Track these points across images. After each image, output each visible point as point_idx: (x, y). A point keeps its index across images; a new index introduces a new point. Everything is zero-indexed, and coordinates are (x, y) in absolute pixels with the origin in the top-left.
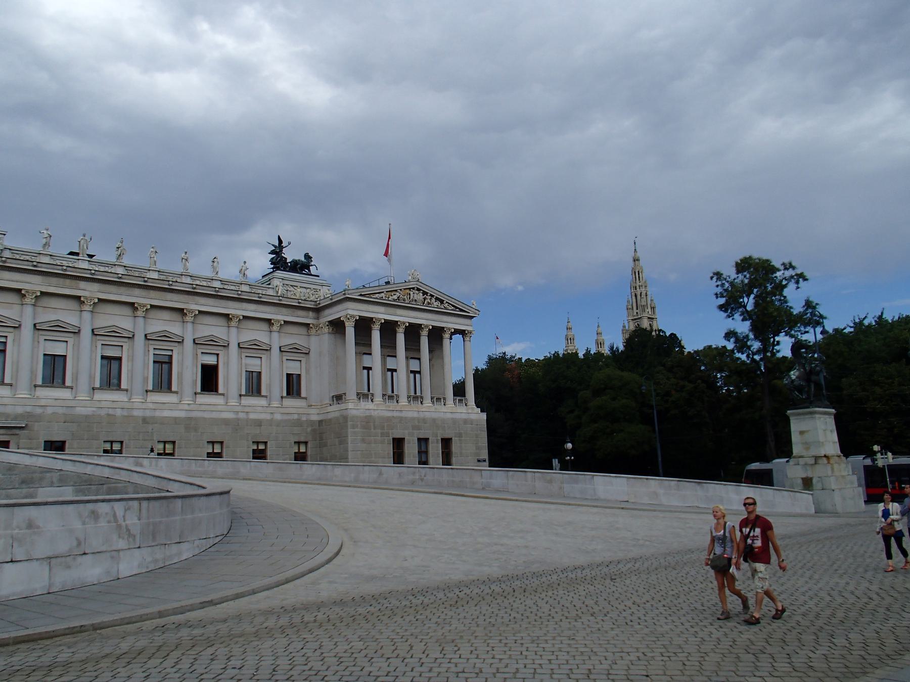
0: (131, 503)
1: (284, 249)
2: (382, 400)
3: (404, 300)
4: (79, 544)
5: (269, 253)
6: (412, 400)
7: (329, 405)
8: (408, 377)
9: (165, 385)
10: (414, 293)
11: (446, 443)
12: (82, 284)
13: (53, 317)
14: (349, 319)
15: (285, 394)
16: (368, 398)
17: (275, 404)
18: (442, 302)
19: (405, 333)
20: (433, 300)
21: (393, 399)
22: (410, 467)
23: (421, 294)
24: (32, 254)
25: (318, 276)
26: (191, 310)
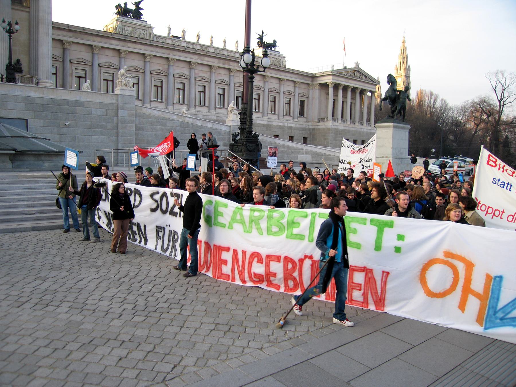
5: (257, 39)
9: (288, 114)
12: (231, 63)
18: (366, 77)
19: (351, 92)
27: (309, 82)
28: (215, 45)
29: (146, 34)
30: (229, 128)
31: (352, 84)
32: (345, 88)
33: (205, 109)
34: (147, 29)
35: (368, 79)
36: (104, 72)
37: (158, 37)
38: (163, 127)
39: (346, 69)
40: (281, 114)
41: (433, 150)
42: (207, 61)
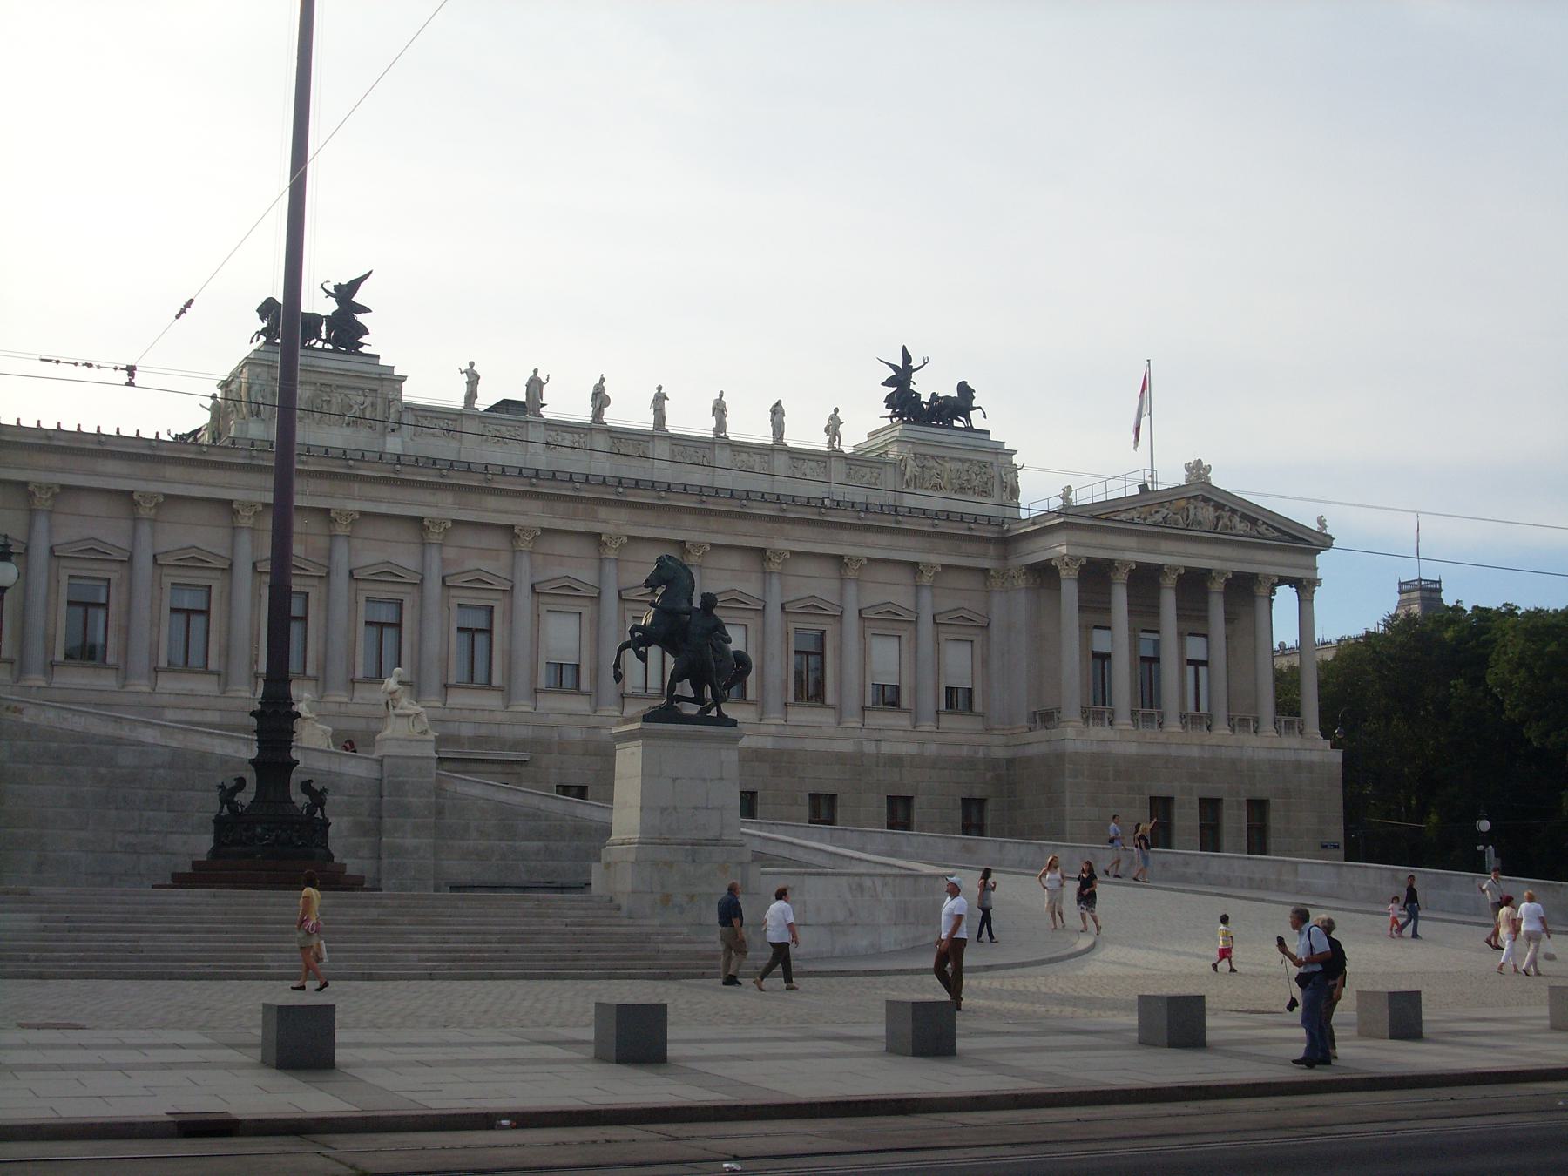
0: (887, 879)
1: (913, 374)
2: (1131, 722)
3: (1176, 522)
4: (851, 915)
5: (883, 384)
6: (1189, 721)
7: (1027, 730)
8: (1182, 673)
10: (1195, 508)
11: (1258, 809)
12: (603, 512)
13: (558, 572)
14: (1067, 565)
15: (943, 706)
16: (1103, 719)
17: (928, 725)
18: (1254, 521)
20: (1236, 519)
21: (1152, 721)
22: (1185, 853)
23: (1211, 509)
24: (448, 416)
25: (988, 432)
26: (779, 550)
27: (986, 564)
28: (674, 425)
29: (373, 405)
30: (376, 766)
31: (1175, 556)
32: (1145, 580)
33: (491, 700)
34: (375, 385)
35: (1263, 529)
36: (70, 576)
37: (427, 416)
38: (103, 770)
39: (1146, 496)
40: (853, 703)
41: (1484, 825)
42: (495, 511)
